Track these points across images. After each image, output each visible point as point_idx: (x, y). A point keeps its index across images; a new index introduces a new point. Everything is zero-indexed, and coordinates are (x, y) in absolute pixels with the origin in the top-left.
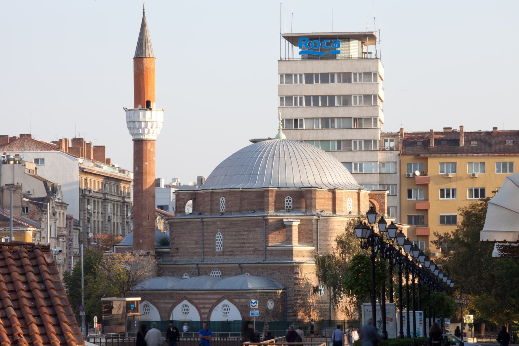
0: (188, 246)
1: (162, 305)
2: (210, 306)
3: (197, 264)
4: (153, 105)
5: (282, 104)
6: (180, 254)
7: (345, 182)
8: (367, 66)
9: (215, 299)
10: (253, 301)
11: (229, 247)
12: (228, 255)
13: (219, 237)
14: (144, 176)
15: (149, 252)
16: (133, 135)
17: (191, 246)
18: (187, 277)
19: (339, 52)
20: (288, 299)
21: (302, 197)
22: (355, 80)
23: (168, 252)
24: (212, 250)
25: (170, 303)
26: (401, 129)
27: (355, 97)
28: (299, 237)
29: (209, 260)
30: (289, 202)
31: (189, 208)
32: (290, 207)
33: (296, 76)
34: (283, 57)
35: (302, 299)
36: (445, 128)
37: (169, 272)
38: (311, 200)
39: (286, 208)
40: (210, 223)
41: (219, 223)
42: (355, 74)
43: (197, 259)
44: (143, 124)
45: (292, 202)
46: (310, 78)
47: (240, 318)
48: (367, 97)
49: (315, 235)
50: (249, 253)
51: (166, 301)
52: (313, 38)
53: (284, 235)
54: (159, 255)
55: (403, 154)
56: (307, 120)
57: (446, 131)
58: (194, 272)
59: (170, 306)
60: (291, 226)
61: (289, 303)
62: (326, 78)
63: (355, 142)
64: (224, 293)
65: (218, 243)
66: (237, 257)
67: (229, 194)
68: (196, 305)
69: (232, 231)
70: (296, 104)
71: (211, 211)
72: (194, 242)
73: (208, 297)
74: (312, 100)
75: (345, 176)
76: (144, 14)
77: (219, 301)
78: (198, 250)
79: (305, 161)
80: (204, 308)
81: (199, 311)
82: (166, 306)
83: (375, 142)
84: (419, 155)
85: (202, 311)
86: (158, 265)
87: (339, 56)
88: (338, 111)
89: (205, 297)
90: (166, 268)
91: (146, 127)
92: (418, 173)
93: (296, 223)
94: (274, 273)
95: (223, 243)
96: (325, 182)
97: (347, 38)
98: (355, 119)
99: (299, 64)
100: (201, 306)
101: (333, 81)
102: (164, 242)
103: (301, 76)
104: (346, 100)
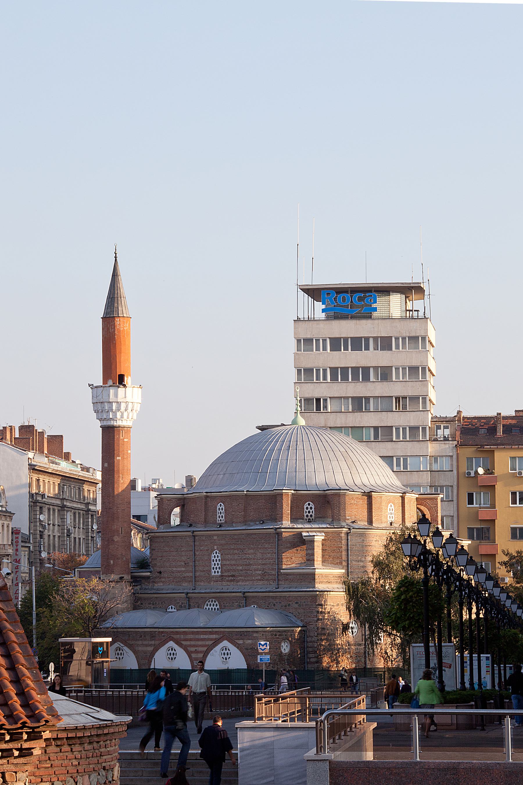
1: (140, 649)
3: (187, 593)
4: (128, 380)
5: (299, 378)
6: (163, 580)
7: (385, 483)
8: (412, 328)
10: (263, 643)
11: (229, 571)
12: (228, 581)
13: (216, 556)
14: (116, 476)
15: (123, 577)
16: (101, 420)
17: (179, 569)
18: (173, 610)
19: (375, 309)
20: (309, 639)
21: (326, 504)
22: (397, 347)
23: (148, 578)
24: (207, 575)
25: (151, 645)
26: (459, 412)
27: (397, 369)
28: (323, 556)
29: (202, 587)
30: (309, 509)
31: (175, 520)
32: (311, 516)
33: (317, 341)
34: (301, 317)
35: (327, 640)
36: (516, 411)
37: (150, 604)
38: (339, 507)
39: (305, 517)
40: (204, 539)
41: (215, 538)
42: (397, 339)
43: (186, 586)
44: (114, 406)
45: (313, 509)
46: (336, 344)
47: (245, 667)
48: (413, 370)
49: (344, 553)
50: (257, 578)
51: (145, 643)
52: (340, 291)
53: (304, 553)
54: (135, 580)
55: (461, 445)
56: (333, 400)
57: (518, 414)
58: (182, 603)
59: (151, 649)
60: (313, 541)
61: (310, 644)
62: (358, 343)
63: (397, 429)
64: (224, 632)
65: (215, 565)
66: (240, 583)
67: (229, 499)
68: (185, 648)
69: (234, 549)
70: (318, 378)
71: (206, 522)
72: (183, 563)
73: (202, 637)
74: (339, 374)
75: (385, 475)
77: (216, 642)
78: (188, 574)
79: (331, 455)
80: (196, 652)
81: (190, 657)
82: (145, 649)
83: (424, 429)
84: (482, 446)
85: (193, 655)
86: (134, 594)
87: (375, 314)
88: (375, 388)
89: (197, 637)
90: (145, 599)
91: (119, 409)
92: (481, 471)
93: (319, 538)
94: (289, 605)
95: (221, 565)
96: (358, 482)
97: (386, 290)
98: (398, 399)
99: (322, 325)
100: (193, 649)
101: (367, 348)
102: (143, 564)
103: (324, 341)
104: (385, 373)
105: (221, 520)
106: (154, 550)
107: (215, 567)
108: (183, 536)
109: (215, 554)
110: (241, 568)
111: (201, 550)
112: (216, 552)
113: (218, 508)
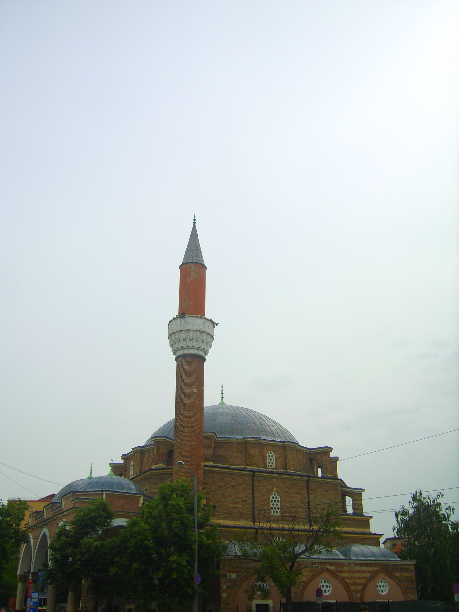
0: (231, 505)
2: (363, 581)
9: (369, 572)
72: (240, 500)
76: (194, 223)
80: (355, 584)
95: (281, 506)
105: (271, 466)
106: (207, 484)
107: (274, 507)
108: (241, 475)
109: (273, 495)
110: (301, 510)
111: (260, 490)
112: (275, 494)
113: (268, 455)
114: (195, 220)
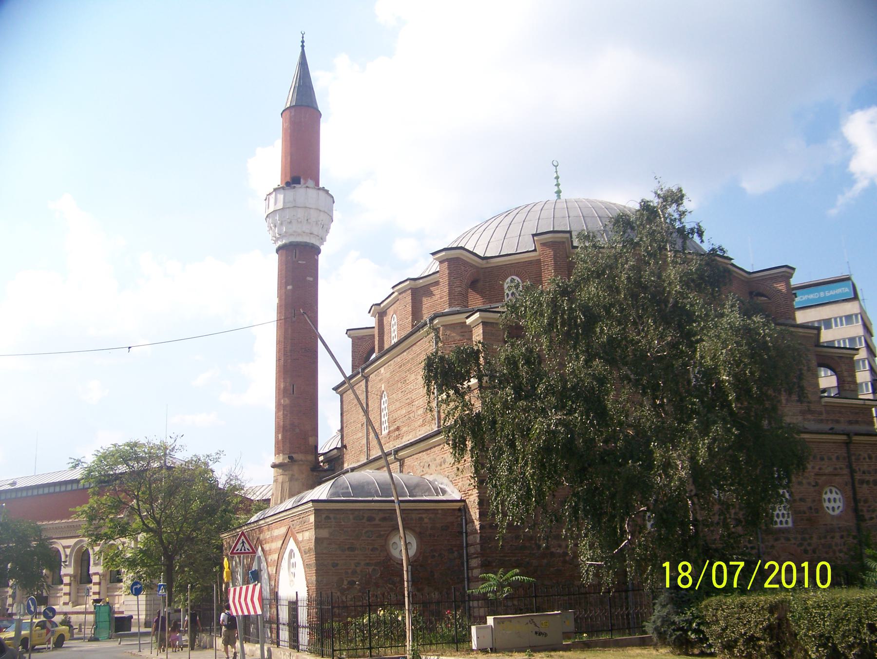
22: (836, 325)
76: (303, 46)
114: (303, 42)
